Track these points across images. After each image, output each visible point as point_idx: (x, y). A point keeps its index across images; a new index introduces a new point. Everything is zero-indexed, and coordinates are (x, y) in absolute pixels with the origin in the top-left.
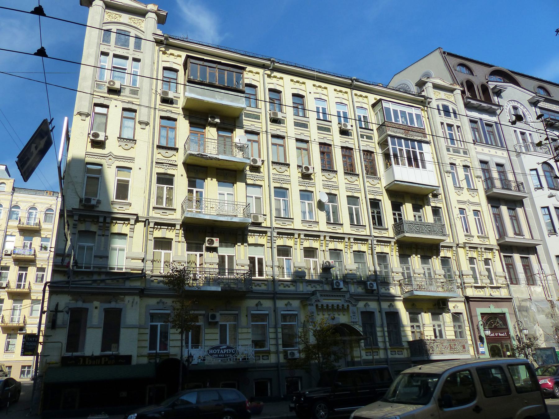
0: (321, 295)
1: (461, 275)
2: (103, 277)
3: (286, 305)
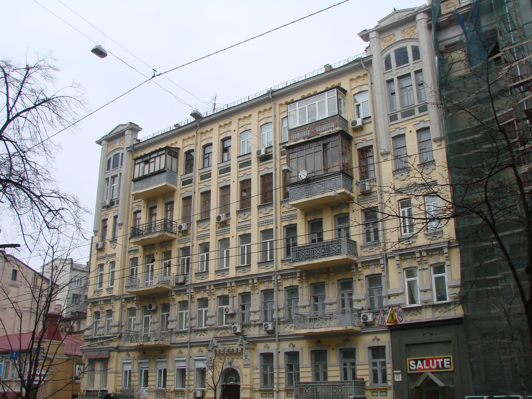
0: (218, 342)
2: (101, 341)
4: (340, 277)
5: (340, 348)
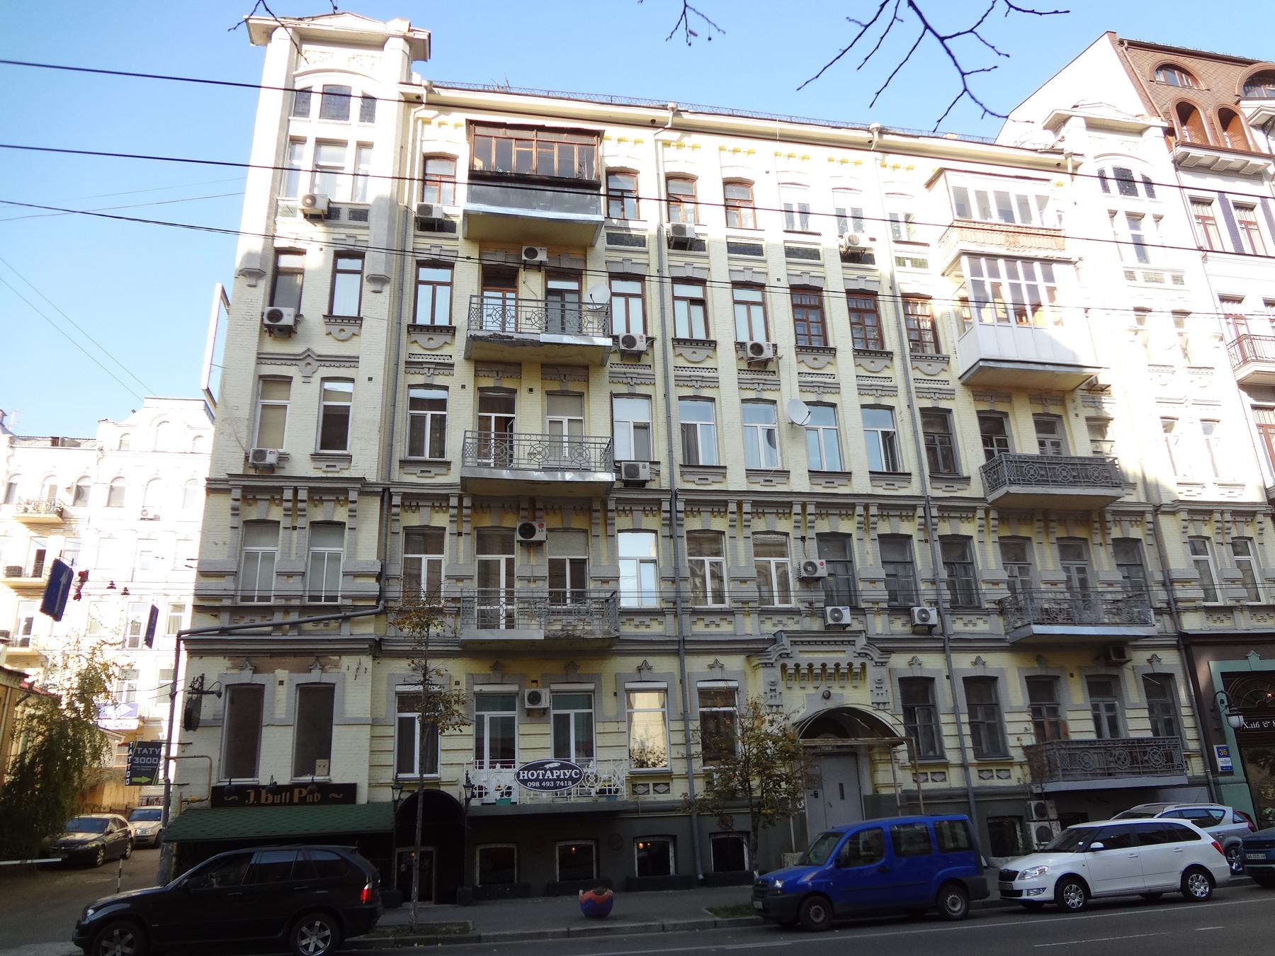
1: (1168, 583)
2: (294, 617)
3: (711, 667)
4: (1062, 534)
5: (1089, 674)
